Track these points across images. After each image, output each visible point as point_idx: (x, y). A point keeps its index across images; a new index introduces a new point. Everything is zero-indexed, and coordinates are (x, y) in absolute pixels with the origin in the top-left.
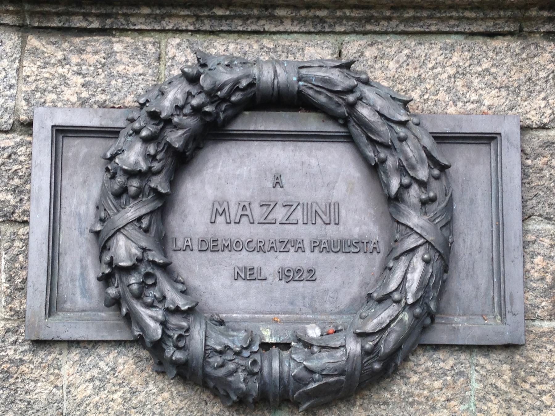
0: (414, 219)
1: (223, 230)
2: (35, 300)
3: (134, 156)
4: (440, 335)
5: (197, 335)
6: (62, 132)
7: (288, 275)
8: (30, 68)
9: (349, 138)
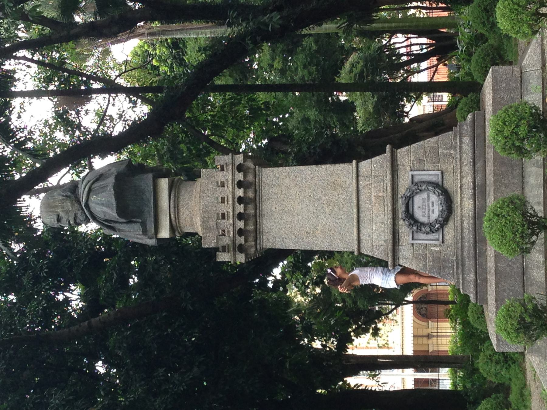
0: (423, 188)
1: (426, 215)
2: (436, 242)
3: (415, 228)
4: (440, 183)
5: (440, 219)
6: (413, 239)
7: (433, 206)
8: (404, 244)
9: (413, 197)
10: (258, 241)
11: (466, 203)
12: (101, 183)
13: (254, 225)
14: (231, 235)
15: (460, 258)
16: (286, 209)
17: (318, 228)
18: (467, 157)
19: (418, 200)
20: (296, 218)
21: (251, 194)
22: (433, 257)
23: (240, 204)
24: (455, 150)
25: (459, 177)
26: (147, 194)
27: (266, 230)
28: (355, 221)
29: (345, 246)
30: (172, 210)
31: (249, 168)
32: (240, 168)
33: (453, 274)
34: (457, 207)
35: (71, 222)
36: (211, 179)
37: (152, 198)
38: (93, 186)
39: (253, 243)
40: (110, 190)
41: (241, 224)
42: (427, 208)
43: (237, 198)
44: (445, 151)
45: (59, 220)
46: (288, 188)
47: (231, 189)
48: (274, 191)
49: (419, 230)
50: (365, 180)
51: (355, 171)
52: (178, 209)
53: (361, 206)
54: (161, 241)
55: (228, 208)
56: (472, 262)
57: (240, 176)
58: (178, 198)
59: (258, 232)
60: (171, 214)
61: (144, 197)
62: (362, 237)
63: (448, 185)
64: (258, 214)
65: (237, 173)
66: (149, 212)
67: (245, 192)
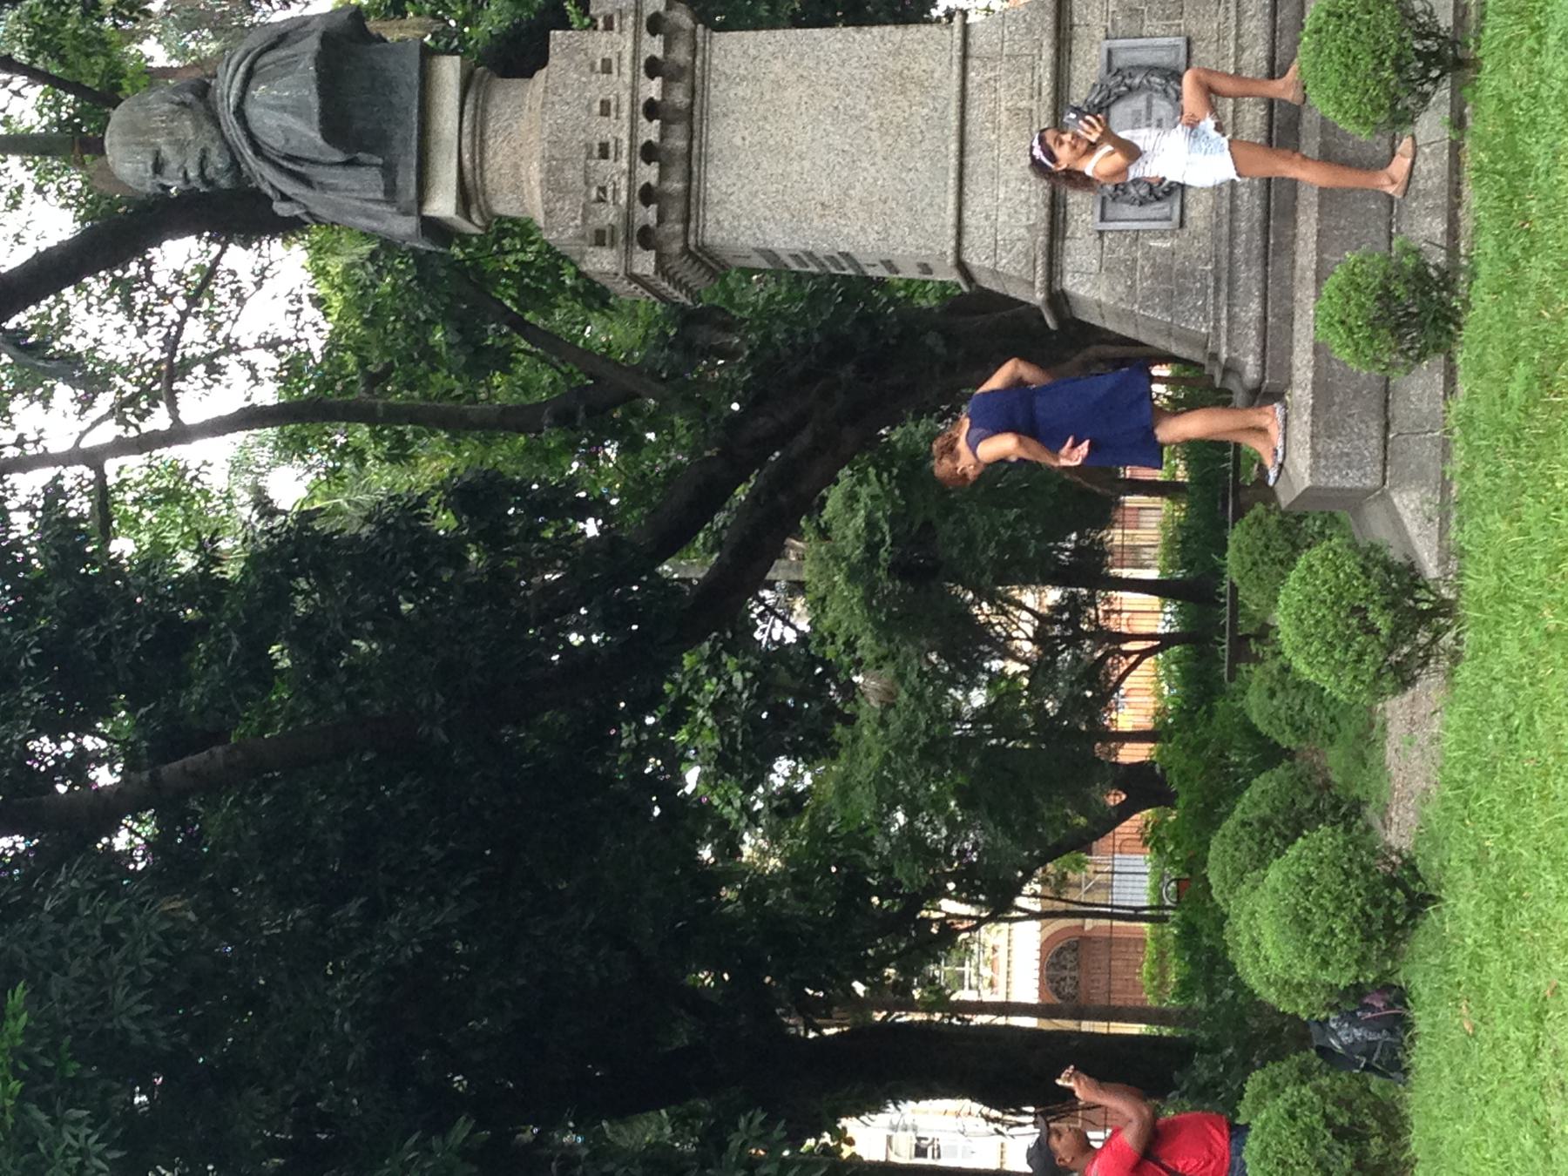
0: (1137, 81)
2: (1165, 225)
6: (1103, 219)
8: (1079, 235)
9: (1108, 107)
10: (692, 225)
11: (1249, 117)
12: (281, 53)
13: (683, 179)
15: (1225, 264)
16: (771, 142)
17: (852, 192)
20: (796, 166)
21: (679, 97)
22: (1153, 265)
23: (650, 120)
25: (1232, 51)
27: (714, 195)
28: (953, 175)
29: (922, 242)
30: (466, 141)
31: (680, 29)
33: (1203, 308)
35: (192, 174)
36: (577, 58)
37: (416, 102)
38: (260, 62)
39: (679, 227)
40: (307, 68)
41: (649, 173)
43: (642, 102)
45: (158, 167)
46: (778, 85)
48: (741, 94)
50: (985, 66)
51: (958, 42)
52: (482, 141)
53: (970, 138)
55: (617, 130)
56: (1256, 270)
57: (654, 46)
58: (484, 110)
59: (693, 200)
60: (464, 150)
61: (395, 100)
64: (695, 151)
65: (646, 36)
67: (665, 90)
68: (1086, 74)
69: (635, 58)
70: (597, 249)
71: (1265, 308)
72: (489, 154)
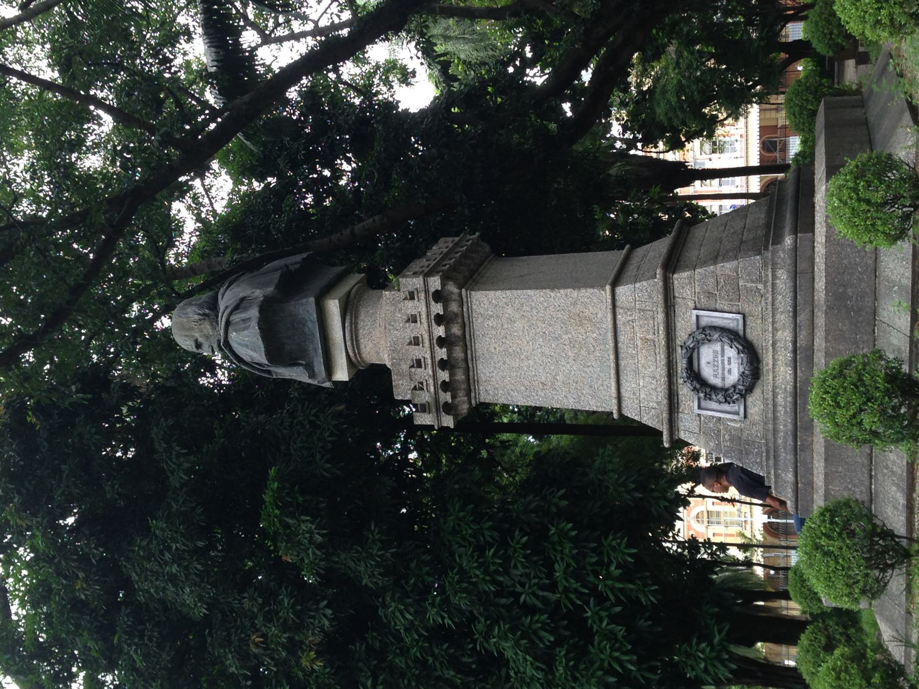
1: (720, 375)
3: (702, 395)
4: (741, 333)
5: (740, 387)
6: (699, 407)
8: (686, 412)
10: (473, 394)
11: (782, 369)
13: (465, 374)
14: (432, 389)
15: (771, 444)
16: (510, 350)
18: (784, 302)
19: (707, 354)
22: (730, 435)
24: (765, 287)
25: (770, 329)
26: (310, 324)
27: (483, 378)
28: (613, 372)
30: (349, 344)
32: (438, 296)
34: (768, 371)
38: (232, 318)
41: (444, 376)
42: (720, 365)
43: (435, 338)
44: (749, 285)
46: (511, 321)
47: (426, 325)
48: (491, 324)
49: (708, 397)
50: (626, 313)
52: (357, 341)
53: (620, 351)
54: (336, 383)
56: (790, 457)
57: (438, 308)
58: (356, 324)
59: (471, 381)
61: (306, 330)
62: (625, 394)
63: (752, 335)
64: (469, 356)
65: (433, 303)
66: (316, 351)
67: (447, 330)
68: (682, 334)
69: (428, 315)
70: (422, 414)
71: (796, 477)
72: (362, 346)
